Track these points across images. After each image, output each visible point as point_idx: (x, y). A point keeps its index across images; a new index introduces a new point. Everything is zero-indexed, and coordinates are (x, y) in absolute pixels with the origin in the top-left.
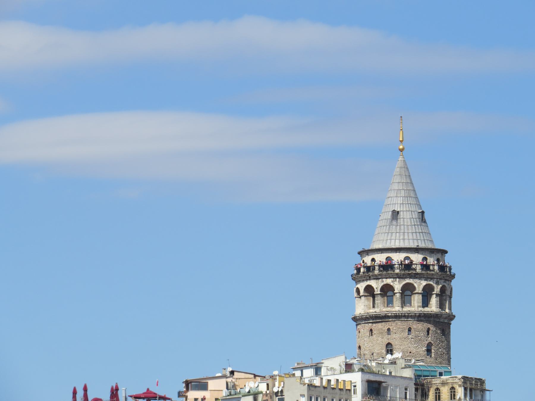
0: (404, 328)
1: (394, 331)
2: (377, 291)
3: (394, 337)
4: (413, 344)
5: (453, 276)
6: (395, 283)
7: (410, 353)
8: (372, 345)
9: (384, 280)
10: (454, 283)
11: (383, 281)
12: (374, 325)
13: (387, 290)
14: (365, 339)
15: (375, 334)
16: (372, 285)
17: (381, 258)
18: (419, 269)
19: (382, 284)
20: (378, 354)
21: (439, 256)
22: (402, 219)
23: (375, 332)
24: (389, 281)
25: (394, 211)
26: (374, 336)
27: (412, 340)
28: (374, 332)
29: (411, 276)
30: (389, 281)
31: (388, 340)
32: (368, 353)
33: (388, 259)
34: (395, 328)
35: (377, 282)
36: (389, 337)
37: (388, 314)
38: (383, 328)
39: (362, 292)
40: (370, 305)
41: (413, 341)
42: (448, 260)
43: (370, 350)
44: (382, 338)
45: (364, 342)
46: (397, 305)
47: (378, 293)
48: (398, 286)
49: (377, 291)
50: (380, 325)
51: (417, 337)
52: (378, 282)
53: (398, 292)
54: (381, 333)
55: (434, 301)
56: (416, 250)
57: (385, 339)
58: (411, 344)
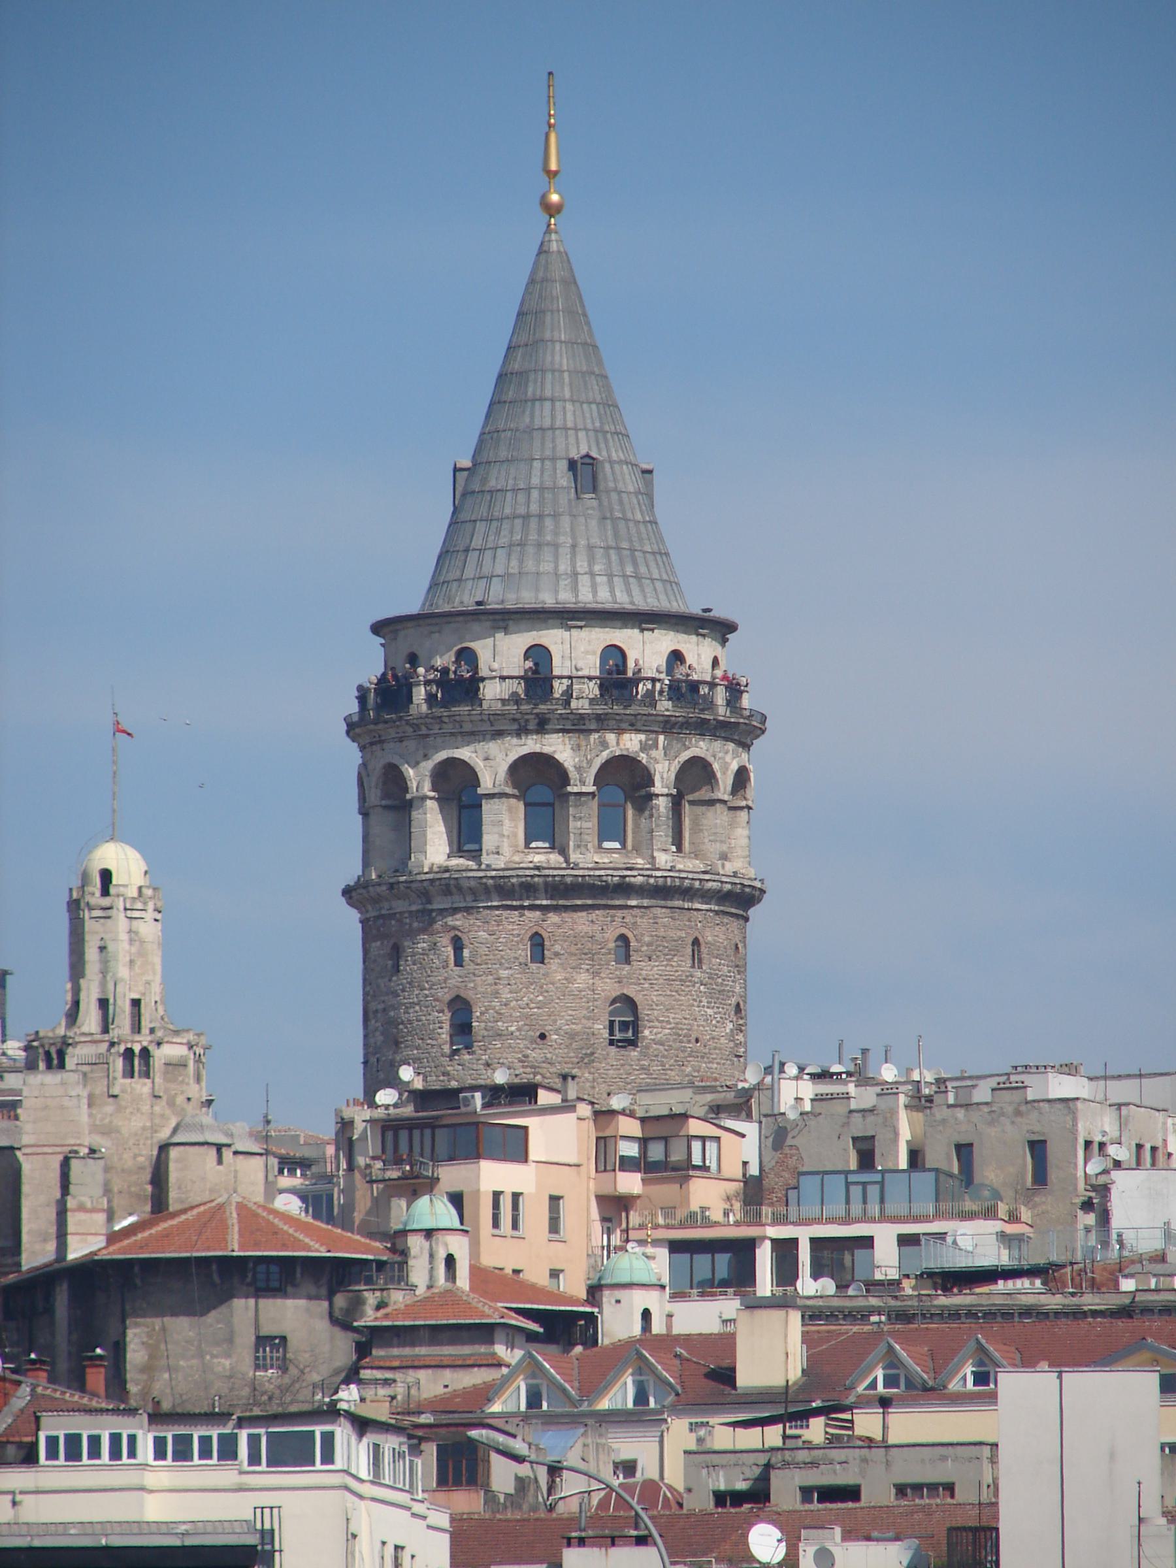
0: (680, 938)
1: (645, 948)
3: (644, 972)
4: (704, 1006)
6: (654, 753)
7: (697, 1041)
8: (541, 998)
9: (611, 737)
11: (604, 745)
12: (553, 918)
14: (504, 973)
15: (557, 954)
16: (556, 756)
19: (605, 755)
20: (572, 1036)
22: (614, 496)
23: (557, 948)
24: (631, 743)
25: (587, 460)
26: (553, 965)
27: (702, 987)
28: (552, 947)
30: (631, 743)
31: (619, 982)
32: (519, 1030)
34: (647, 939)
35: (579, 746)
36: (625, 972)
37: (632, 879)
38: (598, 936)
40: (515, 835)
41: (705, 992)
43: (527, 1017)
44: (596, 974)
45: (496, 984)
46: (659, 846)
47: (585, 789)
49: (583, 783)
50: (581, 922)
51: (713, 979)
52: (583, 743)
53: (665, 791)
54: (586, 954)
57: (608, 980)
58: (699, 1007)
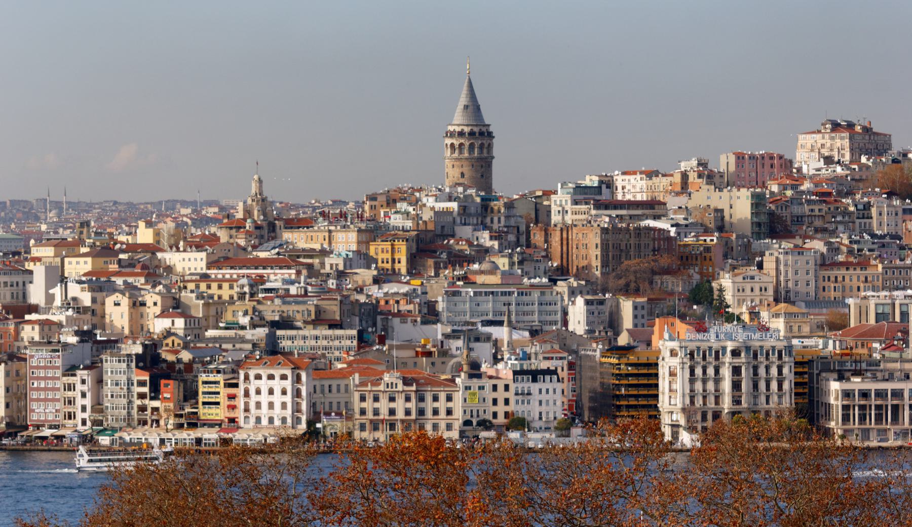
2: (457, 146)
5: (494, 137)
10: (494, 140)
13: (461, 145)
17: (458, 129)
18: (477, 134)
21: (487, 127)
29: (473, 139)
30: (462, 141)
33: (463, 130)
39: (449, 146)
42: (491, 129)
48: (467, 144)
49: (457, 146)
50: (458, 163)
55: (485, 151)
56: (477, 125)
